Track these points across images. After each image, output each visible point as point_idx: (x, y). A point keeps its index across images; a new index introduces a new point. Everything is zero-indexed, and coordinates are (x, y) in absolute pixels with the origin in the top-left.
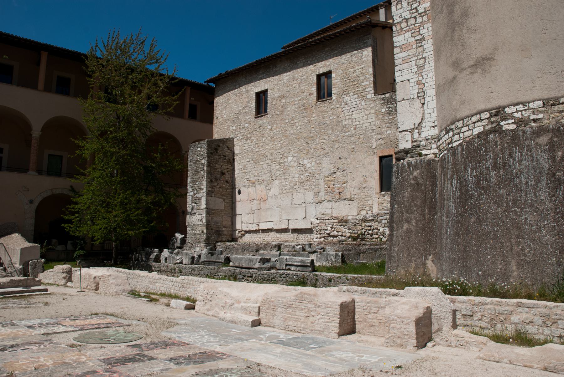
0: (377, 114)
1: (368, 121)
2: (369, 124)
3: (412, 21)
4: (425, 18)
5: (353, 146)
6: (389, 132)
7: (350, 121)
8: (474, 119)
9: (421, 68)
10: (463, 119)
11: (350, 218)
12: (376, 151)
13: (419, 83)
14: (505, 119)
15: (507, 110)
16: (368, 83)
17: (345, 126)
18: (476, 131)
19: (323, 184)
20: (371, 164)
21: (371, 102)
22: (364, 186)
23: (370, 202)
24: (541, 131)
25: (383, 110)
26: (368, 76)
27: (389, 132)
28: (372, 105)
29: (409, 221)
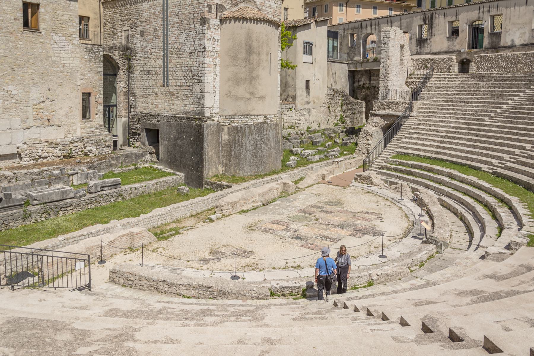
0: (82, 58)
1: (74, 62)
2: (74, 65)
3: (212, 53)
4: (217, 55)
5: (61, 81)
6: (89, 75)
7: (59, 58)
8: (259, 117)
9: (215, 79)
10: (254, 115)
11: (59, 140)
12: (79, 87)
13: (214, 86)
14: (267, 119)
15: (268, 117)
16: (74, 30)
17: (54, 62)
18: (259, 121)
19: (31, 111)
20: (76, 98)
21: (77, 48)
22: (70, 115)
23: (74, 128)
24: (274, 125)
25: (86, 57)
26: (74, 24)
27: (89, 75)
28: (78, 50)
29: (212, 151)
